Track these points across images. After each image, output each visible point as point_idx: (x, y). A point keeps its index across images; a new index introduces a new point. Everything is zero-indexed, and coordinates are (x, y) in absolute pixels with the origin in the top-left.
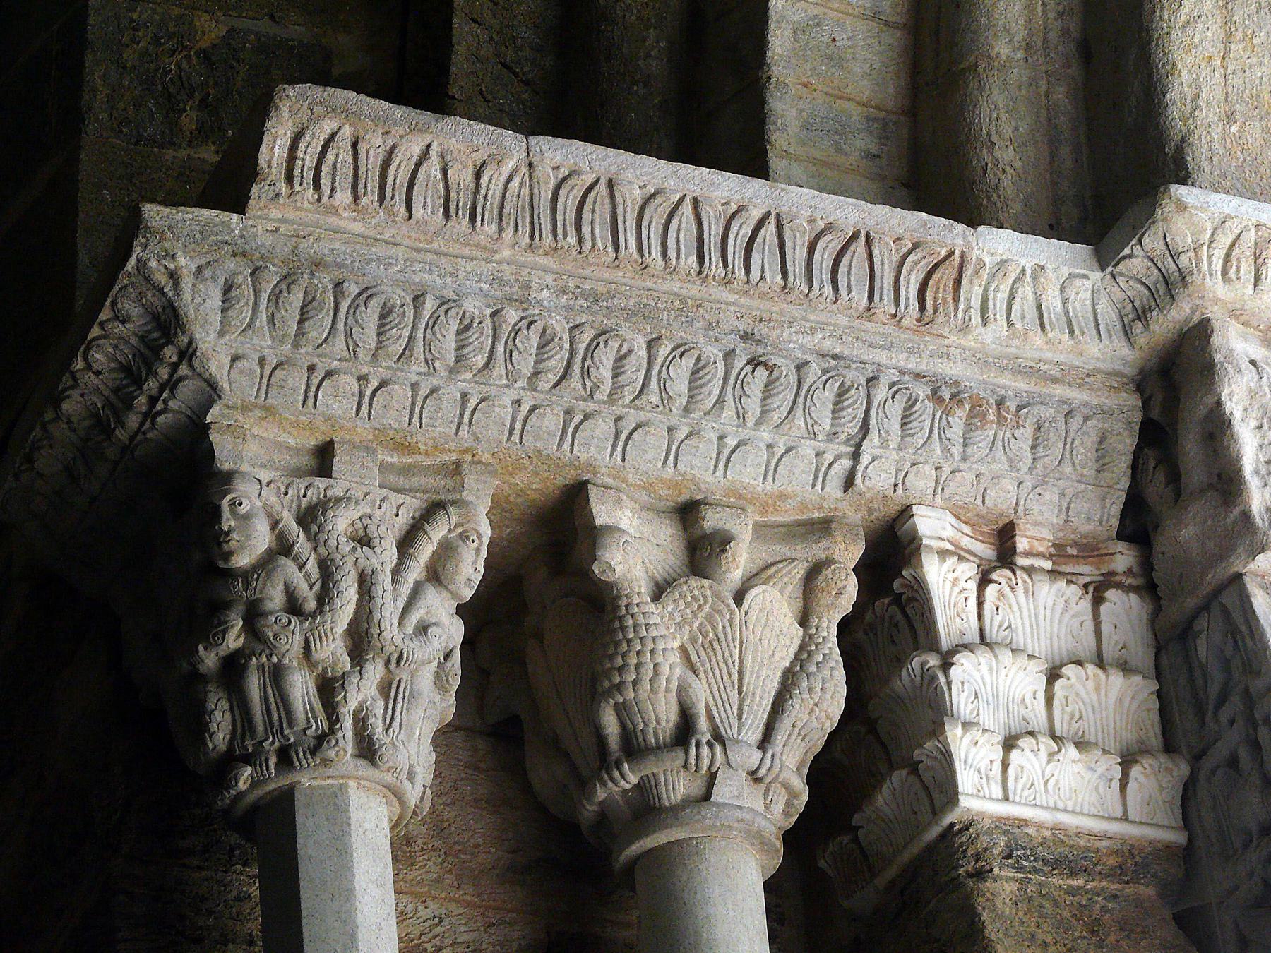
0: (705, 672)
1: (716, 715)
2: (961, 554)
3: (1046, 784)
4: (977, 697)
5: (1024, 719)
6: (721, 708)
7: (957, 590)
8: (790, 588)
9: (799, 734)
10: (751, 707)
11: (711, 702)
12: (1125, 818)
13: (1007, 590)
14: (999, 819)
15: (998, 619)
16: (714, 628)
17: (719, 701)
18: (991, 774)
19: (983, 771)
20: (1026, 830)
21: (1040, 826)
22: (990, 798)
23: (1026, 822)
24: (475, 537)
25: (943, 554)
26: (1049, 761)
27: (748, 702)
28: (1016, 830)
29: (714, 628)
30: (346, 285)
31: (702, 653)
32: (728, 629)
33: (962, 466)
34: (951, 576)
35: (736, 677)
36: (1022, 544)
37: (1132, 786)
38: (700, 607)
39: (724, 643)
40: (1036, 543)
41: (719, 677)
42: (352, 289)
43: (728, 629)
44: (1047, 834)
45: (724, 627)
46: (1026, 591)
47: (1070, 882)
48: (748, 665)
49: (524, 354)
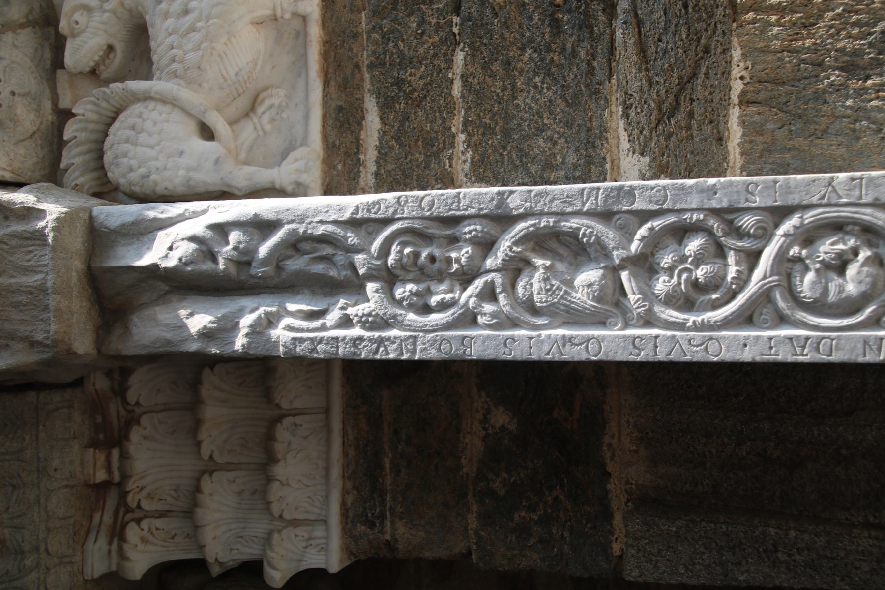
2: (118, 534)
3: (308, 486)
5: (254, 493)
7: (151, 539)
12: (327, 411)
13: (144, 493)
14: (343, 529)
15: (169, 499)
18: (306, 536)
19: (304, 544)
20: (349, 504)
21: (345, 492)
22: (327, 538)
23: (343, 504)
25: (122, 555)
26: (288, 485)
28: (351, 514)
33: (42, 548)
34: (141, 547)
36: (101, 476)
37: (298, 404)
40: (99, 464)
44: (349, 485)
46: (142, 478)
47: (388, 470)
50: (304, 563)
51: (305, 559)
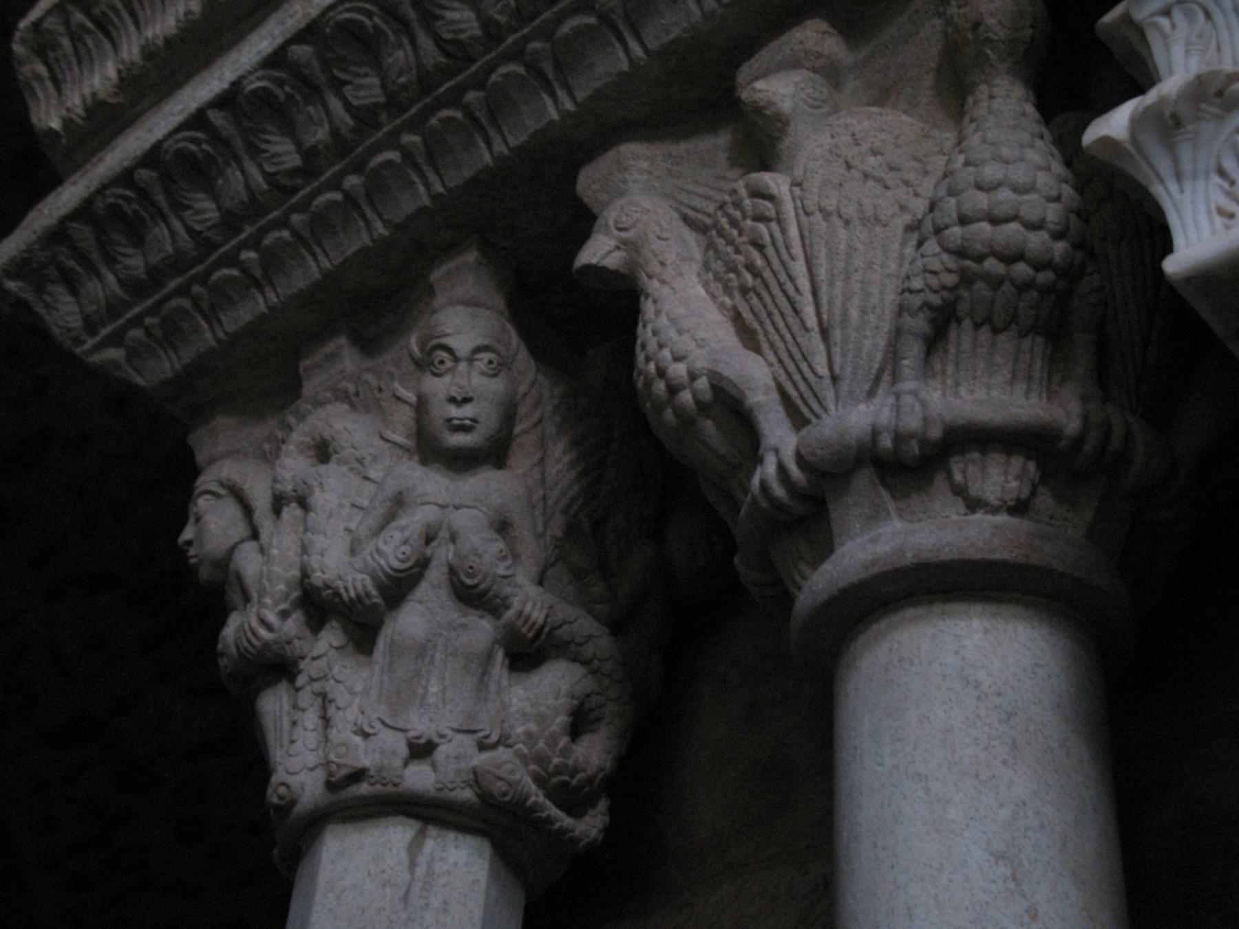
0: (766, 333)
1: (793, 393)
4: (1208, 15)
6: (797, 377)
8: (928, 81)
9: (977, 326)
10: (845, 340)
11: (783, 378)
16: (760, 247)
17: (792, 368)
24: (444, 355)
27: (837, 335)
29: (760, 247)
30: (136, 177)
31: (755, 300)
32: (778, 234)
35: (809, 312)
38: (740, 234)
39: (776, 265)
41: (781, 325)
42: (144, 174)
43: (778, 234)
45: (772, 236)
48: (822, 273)
49: (358, 81)
50: (1173, 187)
51: (1188, 186)
